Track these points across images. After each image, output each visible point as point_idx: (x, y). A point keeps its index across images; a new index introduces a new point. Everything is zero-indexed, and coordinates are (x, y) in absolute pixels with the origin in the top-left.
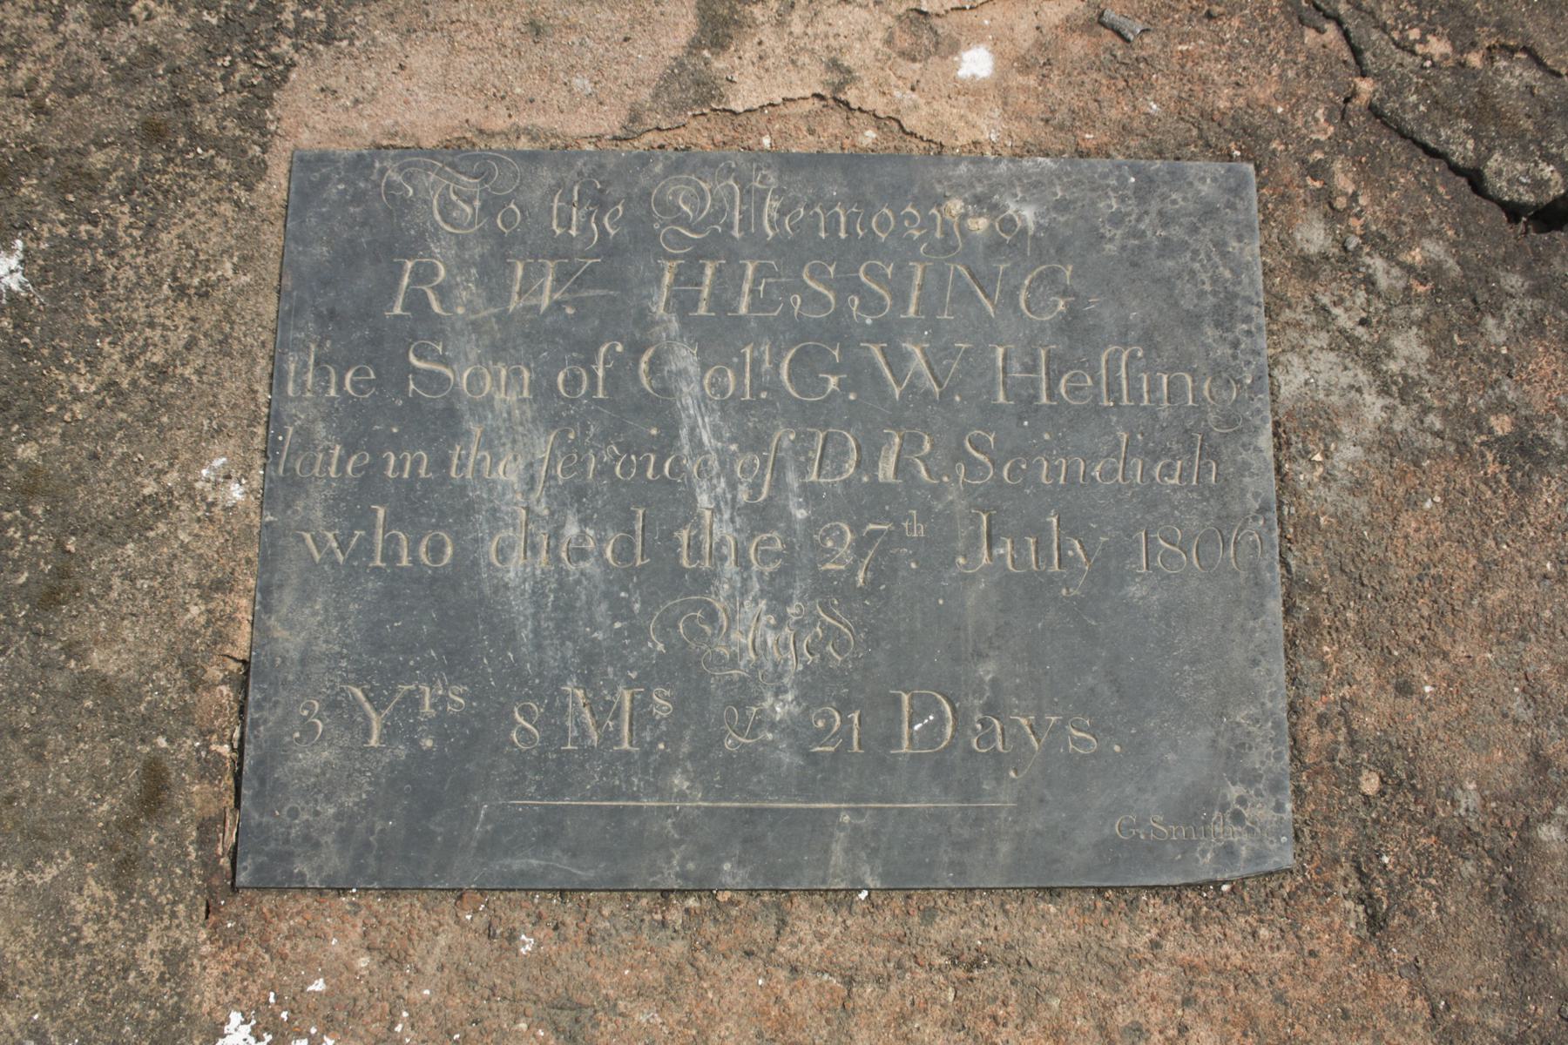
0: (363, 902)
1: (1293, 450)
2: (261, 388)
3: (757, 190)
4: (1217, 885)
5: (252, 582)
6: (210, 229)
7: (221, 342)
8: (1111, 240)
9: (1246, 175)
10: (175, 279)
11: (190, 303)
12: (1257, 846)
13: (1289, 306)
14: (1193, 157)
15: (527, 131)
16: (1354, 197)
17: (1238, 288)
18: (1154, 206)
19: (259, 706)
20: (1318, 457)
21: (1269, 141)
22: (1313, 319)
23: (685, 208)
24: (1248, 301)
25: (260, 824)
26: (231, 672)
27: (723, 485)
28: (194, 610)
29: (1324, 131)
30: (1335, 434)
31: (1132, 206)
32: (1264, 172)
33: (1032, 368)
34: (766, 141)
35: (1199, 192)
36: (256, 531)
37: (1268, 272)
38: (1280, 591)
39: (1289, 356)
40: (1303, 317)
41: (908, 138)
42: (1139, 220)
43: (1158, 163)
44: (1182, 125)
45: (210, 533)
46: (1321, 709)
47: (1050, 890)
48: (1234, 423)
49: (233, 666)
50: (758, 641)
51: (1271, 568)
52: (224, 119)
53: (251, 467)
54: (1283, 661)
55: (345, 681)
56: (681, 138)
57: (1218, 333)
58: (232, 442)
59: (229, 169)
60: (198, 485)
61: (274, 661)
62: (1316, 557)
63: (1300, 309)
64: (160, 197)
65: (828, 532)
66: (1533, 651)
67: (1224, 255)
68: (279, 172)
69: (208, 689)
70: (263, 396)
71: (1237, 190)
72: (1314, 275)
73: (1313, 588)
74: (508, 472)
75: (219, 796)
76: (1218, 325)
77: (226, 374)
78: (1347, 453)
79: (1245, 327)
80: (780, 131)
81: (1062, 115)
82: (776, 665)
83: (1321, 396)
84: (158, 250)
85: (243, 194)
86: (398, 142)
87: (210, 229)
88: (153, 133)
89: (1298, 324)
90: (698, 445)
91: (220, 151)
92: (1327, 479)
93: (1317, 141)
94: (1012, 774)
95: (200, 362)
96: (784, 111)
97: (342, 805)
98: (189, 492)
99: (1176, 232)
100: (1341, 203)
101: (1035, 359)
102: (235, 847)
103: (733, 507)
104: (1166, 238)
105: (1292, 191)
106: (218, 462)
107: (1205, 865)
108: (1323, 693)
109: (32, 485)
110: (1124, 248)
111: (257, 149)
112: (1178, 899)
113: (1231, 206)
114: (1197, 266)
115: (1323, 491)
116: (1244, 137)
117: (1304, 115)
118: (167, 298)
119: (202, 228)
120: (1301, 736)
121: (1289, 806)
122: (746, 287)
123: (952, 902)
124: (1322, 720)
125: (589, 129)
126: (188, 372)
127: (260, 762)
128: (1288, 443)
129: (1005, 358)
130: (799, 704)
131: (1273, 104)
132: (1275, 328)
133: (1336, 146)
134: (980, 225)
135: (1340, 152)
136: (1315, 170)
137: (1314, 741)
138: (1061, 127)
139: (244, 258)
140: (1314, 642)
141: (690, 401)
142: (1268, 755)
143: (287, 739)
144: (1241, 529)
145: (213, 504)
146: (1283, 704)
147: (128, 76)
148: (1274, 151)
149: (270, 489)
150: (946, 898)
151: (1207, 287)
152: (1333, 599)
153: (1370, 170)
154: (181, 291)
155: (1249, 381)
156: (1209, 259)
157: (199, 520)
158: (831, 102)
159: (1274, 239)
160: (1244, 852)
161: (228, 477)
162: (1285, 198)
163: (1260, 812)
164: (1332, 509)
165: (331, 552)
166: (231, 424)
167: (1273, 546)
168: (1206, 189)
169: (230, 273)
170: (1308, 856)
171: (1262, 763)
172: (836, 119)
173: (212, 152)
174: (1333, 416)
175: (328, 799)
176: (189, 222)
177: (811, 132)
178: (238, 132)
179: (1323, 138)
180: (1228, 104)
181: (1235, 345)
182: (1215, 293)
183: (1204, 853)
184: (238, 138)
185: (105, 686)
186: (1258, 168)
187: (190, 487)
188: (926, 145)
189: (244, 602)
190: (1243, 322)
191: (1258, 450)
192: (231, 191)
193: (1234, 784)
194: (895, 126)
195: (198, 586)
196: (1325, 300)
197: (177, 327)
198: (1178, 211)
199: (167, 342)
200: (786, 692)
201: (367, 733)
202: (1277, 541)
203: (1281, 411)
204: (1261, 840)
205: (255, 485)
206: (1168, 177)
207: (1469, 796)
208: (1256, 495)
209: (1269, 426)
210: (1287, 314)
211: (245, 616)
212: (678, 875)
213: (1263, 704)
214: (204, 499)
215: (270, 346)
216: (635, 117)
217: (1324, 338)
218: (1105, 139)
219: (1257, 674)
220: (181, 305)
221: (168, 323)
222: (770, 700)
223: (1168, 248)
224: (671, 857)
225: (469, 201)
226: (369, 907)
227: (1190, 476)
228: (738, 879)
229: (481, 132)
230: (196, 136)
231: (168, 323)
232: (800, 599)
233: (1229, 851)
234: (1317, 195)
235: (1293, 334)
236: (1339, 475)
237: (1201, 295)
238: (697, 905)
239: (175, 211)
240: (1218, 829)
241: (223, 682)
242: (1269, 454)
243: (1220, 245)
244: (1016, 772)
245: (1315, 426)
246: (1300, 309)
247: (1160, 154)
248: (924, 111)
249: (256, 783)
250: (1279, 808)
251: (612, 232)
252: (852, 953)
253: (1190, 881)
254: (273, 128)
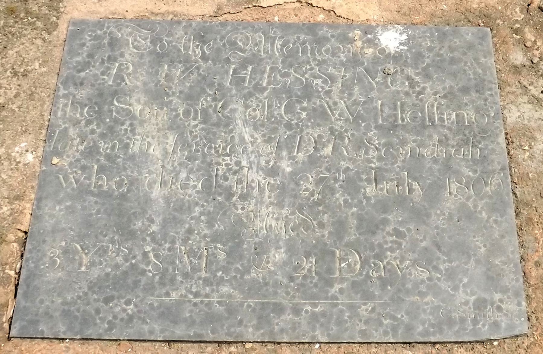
0: (71, 346)
1: (514, 145)
2: (46, 114)
3: (272, 37)
4: (491, 341)
5: (33, 196)
6: (31, 50)
7: (30, 95)
8: (428, 57)
9: (486, 32)
10: (13, 69)
11: (18, 79)
12: (509, 322)
13: (509, 85)
14: (463, 25)
15: (173, 13)
16: (535, 42)
17: (485, 77)
18: (446, 44)
19: (30, 251)
20: (526, 148)
21: (496, 20)
22: (520, 91)
23: (240, 44)
24: (491, 82)
25: (24, 307)
26: (19, 237)
27: (253, 156)
28: (5, 209)
29: (520, 17)
30: (534, 138)
31: (437, 45)
32: (495, 32)
33: (395, 109)
34: (276, 19)
35: (467, 38)
36: (37, 174)
37: (499, 71)
38: (514, 206)
39: (510, 105)
40: (516, 90)
41: (338, 18)
42: (440, 49)
43: (448, 27)
44: (457, 14)
45: (16, 175)
46: (536, 259)
47: (409, 343)
48: (487, 133)
49: (21, 235)
50: (268, 226)
51: (508, 194)
52: (41, 7)
53: (38, 147)
54: (517, 237)
55: (72, 240)
56: (239, 17)
57: (478, 95)
58: (31, 136)
59: (42, 26)
60: (13, 154)
61: (39, 232)
62: (528, 191)
63: (514, 86)
64: (10, 37)
65: (301, 178)
67: (479, 64)
69: (7, 244)
70: (47, 117)
71: (483, 38)
72: (519, 73)
73: (527, 204)
74: (155, 151)
75: (7, 294)
76: (477, 91)
77: (31, 108)
79: (489, 92)
80: (283, 15)
81: (405, 9)
82: (276, 236)
83: (526, 122)
84: (7, 57)
85: (47, 36)
86: (116, 16)
87: (31, 50)
89: (513, 93)
90: (242, 139)
91: (38, 18)
92: (532, 157)
93: (517, 20)
94: (389, 287)
95: (20, 103)
96: (284, 7)
97: (65, 298)
98: (9, 157)
99: (456, 54)
100: (529, 44)
101: (395, 105)
102: (12, 318)
103: (258, 167)
104: (452, 57)
105: (507, 39)
106: (23, 145)
107: (485, 333)
108: (537, 251)
110: (434, 61)
111: (55, 18)
112: (473, 349)
113: (480, 44)
114: (467, 68)
115: (529, 162)
117: (511, 10)
118: (8, 77)
119: (27, 49)
120: (527, 271)
121: (524, 304)
122: (266, 76)
123: (361, 350)
124: (537, 264)
125: (199, 13)
126: (14, 107)
127: (28, 277)
128: (512, 142)
129: (382, 105)
130: (287, 254)
131: (497, 6)
132: (503, 94)
133: (526, 22)
134: (369, 51)
135: (527, 25)
136: (516, 31)
137: (534, 273)
138: (405, 14)
139: (44, 61)
140: (531, 229)
141: (239, 122)
142: (512, 280)
143: (42, 267)
144: (492, 178)
145: (19, 162)
146: (518, 256)
148: (498, 24)
149: (46, 156)
150: (358, 348)
151: (472, 76)
152: (538, 209)
154: (15, 74)
155: (493, 115)
156: (472, 65)
157: (12, 169)
158: (305, 4)
159: (500, 58)
160: (503, 325)
161: (27, 151)
162: (504, 42)
163: (510, 306)
164: (535, 170)
165: (71, 183)
166: (31, 129)
167: (508, 185)
168: (469, 38)
169: (37, 67)
170: (535, 329)
171: (510, 283)
172: (306, 11)
173: (35, 19)
174: (532, 131)
175: (59, 295)
176: (22, 46)
177: (296, 15)
178: (47, 12)
179: (519, 19)
180: (477, 6)
181: (486, 100)
182: (475, 79)
183: (484, 325)
184: (47, 14)
186: (491, 30)
187: (9, 155)
188: (346, 21)
189: (28, 205)
190: (489, 90)
191: (498, 144)
192: (41, 34)
193: (496, 293)
194: (332, 12)
195: (8, 198)
196: (525, 83)
197: (11, 89)
198: (457, 46)
199: (6, 94)
200: (281, 248)
201: (80, 265)
202: (510, 184)
203: (508, 128)
204: (511, 320)
205: (39, 154)
206: (452, 33)
208: (499, 163)
209: (503, 133)
210: (508, 89)
211: (28, 211)
212: (227, 334)
213: (508, 256)
214: (15, 160)
215: (52, 96)
216: (219, 8)
217: (526, 99)
218: (424, 19)
219: (504, 241)
220: (14, 79)
221: (8, 86)
222: (273, 252)
223: (453, 61)
224: (224, 325)
225: (145, 39)
226: (74, 349)
227: (467, 155)
228: (256, 337)
229: (152, 13)
230: (28, 13)
231: (8, 86)
232: (289, 206)
233: (496, 325)
234: (518, 41)
235: (511, 97)
236: (537, 156)
237: (469, 80)
238: (235, 350)
239: (16, 42)
240: (491, 314)
241: (15, 242)
242: (504, 145)
243: (476, 59)
244: (391, 286)
245: (524, 135)
246: (514, 86)
247: (448, 25)
248: (345, 7)
249: (25, 287)
250: (519, 304)
251: (207, 53)
253: (478, 339)
254: (62, 10)
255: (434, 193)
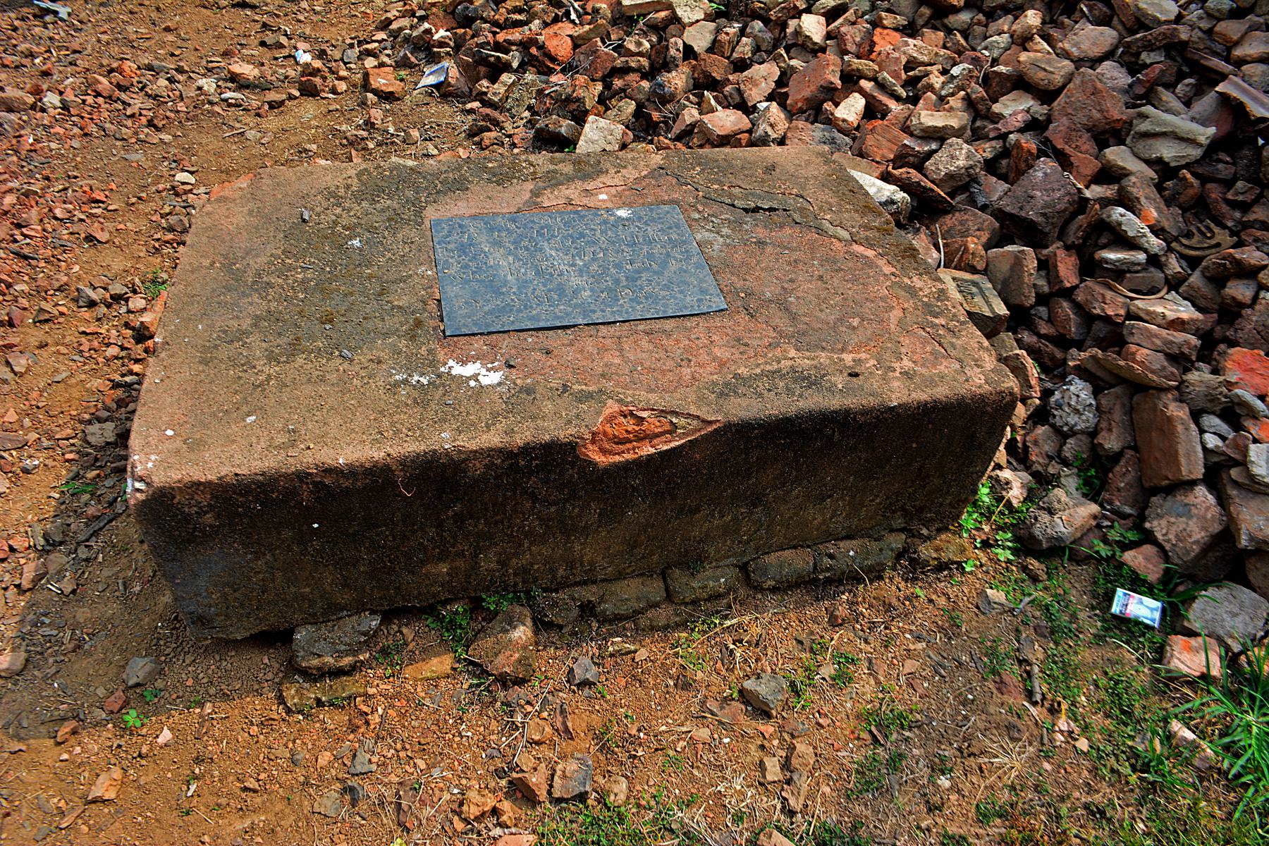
66: (775, 273)
68: (427, 223)
78: (716, 247)
88: (389, 220)
107: (705, 310)
109: (370, 277)
116: (673, 202)
147: (383, 211)
153: (705, 205)
163: (717, 299)
185: (400, 307)
207: (768, 294)
252: (618, 334)
255: (664, 265)
